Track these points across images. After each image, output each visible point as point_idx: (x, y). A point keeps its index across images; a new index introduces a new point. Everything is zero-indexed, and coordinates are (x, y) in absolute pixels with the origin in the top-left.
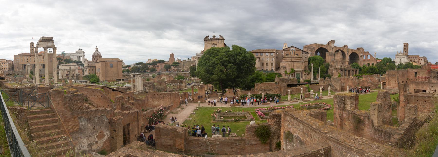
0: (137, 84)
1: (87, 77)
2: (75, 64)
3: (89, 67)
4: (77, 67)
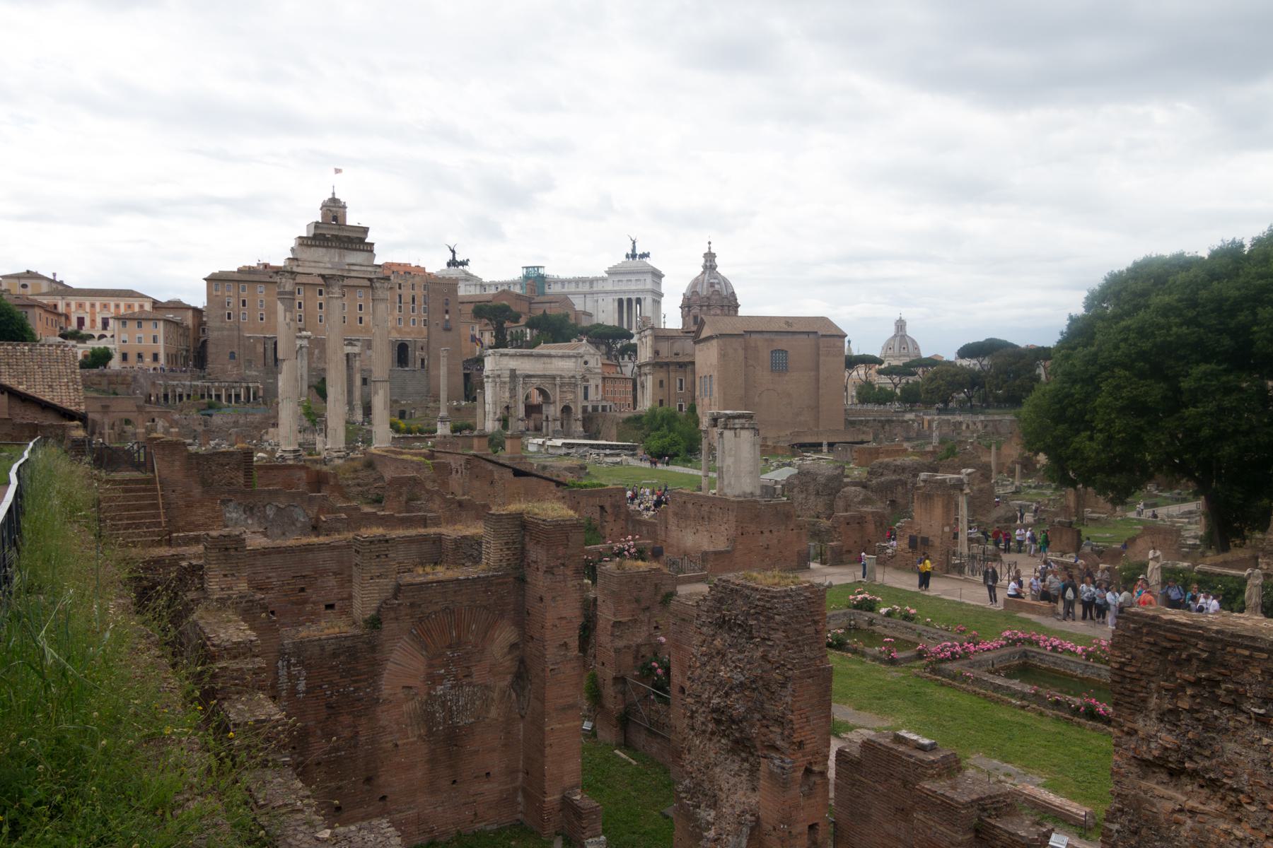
0: (729, 461)
1: (636, 421)
2: (584, 347)
3: (658, 364)
4: (596, 359)
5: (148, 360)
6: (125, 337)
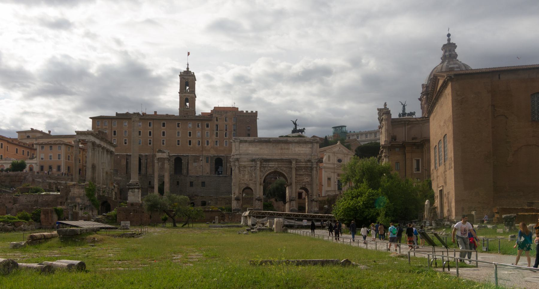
5: (54, 170)
6: (42, 156)
